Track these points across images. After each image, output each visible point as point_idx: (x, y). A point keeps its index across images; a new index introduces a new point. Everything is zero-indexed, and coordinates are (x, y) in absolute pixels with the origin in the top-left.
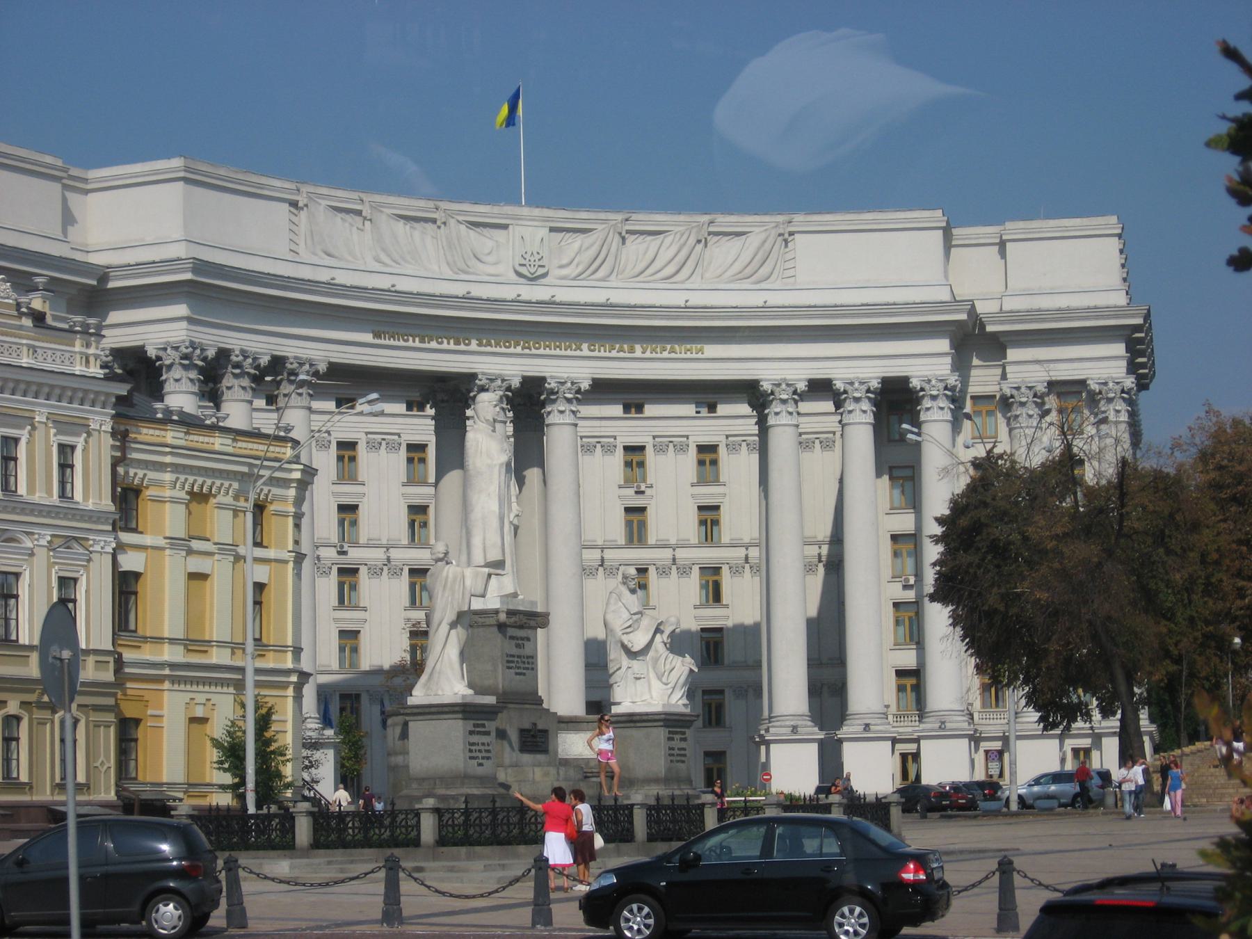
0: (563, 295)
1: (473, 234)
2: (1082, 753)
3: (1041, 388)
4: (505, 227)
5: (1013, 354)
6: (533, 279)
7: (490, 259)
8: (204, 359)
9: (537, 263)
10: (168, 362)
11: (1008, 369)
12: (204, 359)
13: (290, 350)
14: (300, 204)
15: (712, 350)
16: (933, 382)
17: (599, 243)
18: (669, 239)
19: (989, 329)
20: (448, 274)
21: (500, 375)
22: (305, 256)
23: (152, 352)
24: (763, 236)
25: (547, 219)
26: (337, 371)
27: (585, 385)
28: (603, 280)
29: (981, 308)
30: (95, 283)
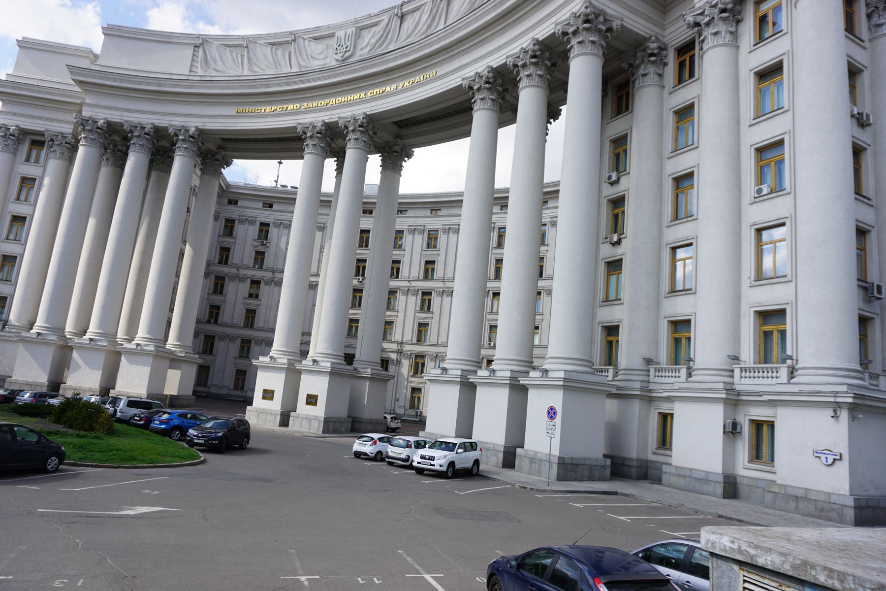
1: (312, 44)
2: (765, 429)
4: (332, 36)
7: (322, 56)
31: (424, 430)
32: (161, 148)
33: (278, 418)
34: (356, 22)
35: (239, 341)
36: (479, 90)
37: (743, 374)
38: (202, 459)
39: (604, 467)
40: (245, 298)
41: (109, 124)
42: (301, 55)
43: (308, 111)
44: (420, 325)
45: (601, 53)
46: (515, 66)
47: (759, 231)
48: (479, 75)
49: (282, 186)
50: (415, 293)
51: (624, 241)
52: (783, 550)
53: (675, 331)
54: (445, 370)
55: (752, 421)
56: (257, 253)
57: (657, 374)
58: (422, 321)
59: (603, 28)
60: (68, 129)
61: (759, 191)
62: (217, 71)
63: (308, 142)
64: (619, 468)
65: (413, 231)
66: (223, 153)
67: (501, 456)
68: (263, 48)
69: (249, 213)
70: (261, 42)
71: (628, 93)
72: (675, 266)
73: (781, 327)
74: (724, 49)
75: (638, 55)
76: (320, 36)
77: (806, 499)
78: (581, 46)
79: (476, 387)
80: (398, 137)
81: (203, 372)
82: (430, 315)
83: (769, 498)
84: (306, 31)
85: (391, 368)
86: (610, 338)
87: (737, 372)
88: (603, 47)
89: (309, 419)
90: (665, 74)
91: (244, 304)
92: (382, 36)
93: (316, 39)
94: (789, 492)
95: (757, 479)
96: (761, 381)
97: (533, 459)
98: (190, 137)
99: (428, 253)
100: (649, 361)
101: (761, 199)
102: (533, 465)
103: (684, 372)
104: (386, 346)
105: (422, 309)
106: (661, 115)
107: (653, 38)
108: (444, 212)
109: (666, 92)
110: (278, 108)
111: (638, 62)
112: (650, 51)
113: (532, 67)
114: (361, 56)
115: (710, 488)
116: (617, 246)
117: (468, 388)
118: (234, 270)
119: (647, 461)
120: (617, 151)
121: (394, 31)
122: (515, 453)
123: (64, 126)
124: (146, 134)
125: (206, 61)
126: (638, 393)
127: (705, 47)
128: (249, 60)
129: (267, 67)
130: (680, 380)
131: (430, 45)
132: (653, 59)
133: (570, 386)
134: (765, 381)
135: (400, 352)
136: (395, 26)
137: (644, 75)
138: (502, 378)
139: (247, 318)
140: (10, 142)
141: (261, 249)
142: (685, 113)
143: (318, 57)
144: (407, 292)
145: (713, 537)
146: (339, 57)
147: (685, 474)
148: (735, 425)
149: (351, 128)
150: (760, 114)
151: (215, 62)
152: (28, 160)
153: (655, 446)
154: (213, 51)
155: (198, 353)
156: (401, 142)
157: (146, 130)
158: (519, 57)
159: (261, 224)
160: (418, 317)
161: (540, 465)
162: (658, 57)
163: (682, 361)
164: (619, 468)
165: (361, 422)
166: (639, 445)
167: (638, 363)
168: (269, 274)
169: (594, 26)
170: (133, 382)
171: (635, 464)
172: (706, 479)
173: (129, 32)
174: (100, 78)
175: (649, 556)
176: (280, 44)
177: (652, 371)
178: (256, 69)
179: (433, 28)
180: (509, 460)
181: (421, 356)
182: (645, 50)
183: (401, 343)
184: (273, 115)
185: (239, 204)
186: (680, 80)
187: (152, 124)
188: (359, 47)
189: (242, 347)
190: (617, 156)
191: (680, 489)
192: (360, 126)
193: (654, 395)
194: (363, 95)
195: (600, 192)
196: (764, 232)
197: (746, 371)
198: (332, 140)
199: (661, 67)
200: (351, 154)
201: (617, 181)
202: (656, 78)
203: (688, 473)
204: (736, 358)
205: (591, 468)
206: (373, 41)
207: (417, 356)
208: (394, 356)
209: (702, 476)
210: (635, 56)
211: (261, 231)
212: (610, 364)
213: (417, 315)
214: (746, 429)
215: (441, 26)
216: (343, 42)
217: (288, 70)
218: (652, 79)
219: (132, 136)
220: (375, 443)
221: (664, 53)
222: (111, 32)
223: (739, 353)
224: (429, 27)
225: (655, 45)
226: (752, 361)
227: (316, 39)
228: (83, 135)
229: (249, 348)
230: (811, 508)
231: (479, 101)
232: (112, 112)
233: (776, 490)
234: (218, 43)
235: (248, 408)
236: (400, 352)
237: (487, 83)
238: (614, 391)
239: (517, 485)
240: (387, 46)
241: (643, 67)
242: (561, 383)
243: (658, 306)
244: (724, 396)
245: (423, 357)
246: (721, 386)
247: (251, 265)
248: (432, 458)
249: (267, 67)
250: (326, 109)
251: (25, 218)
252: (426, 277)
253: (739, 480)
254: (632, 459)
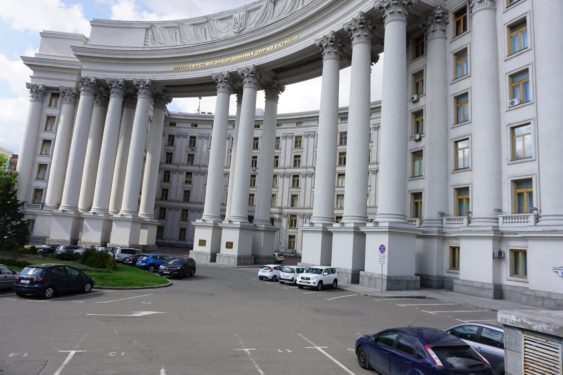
1: (219, 23)
2: (520, 255)
4: (231, 17)
21: (221, 73)
31: (300, 262)
32: (129, 94)
33: (209, 257)
34: (246, 7)
35: (181, 210)
36: (326, 46)
37: (505, 221)
38: (170, 283)
39: (416, 281)
40: (183, 184)
41: (97, 80)
42: (212, 31)
43: (218, 65)
44: (293, 196)
45: (405, 19)
46: (349, 30)
47: (513, 129)
48: (326, 37)
49: (202, 113)
50: (289, 176)
51: (423, 138)
52: (548, 322)
53: (459, 195)
54: (312, 224)
55: (511, 250)
56: (189, 155)
57: (448, 222)
58: (294, 194)
59: (406, 3)
60: (73, 85)
61: (512, 103)
62: (161, 44)
63: (219, 85)
64: (425, 282)
65: (286, 137)
66: (166, 94)
67: (350, 276)
68: (189, 27)
69: (183, 131)
70: (187, 24)
71: (423, 44)
72: (458, 153)
73: (529, 190)
74: (486, 11)
75: (429, 18)
76: (223, 18)
77: (549, 298)
78: (392, 15)
79: (365, 235)
80: (275, 78)
81: (160, 229)
82: (298, 190)
83: (524, 298)
84: (215, 15)
85: (276, 224)
86: (416, 201)
87: (501, 219)
88: (406, 15)
89: (229, 256)
90: (448, 30)
91: (183, 187)
92: (262, 16)
93: (221, 20)
94: (538, 294)
95: (516, 287)
96: (517, 225)
97: (371, 278)
98: (147, 86)
99: (296, 150)
100: (442, 214)
101: (514, 108)
102: (371, 281)
103: (465, 220)
104: (273, 210)
105: (293, 186)
106: (445, 56)
107: (439, 7)
108: (305, 124)
109: (448, 41)
110: (199, 65)
111: (429, 23)
112: (437, 16)
113: (360, 30)
114: (250, 29)
115: (485, 293)
116: (419, 142)
117: (327, 235)
118: (176, 167)
119: (443, 277)
120: (417, 81)
121: (270, 12)
122: (359, 274)
123: (68, 83)
124: (120, 85)
126: (436, 234)
127: (474, 11)
128: (180, 36)
129: (192, 39)
130: (463, 225)
131: (294, 19)
132: (439, 20)
133: (393, 231)
134: (519, 225)
135: (281, 214)
136: (271, 9)
137: (434, 31)
138: (349, 228)
139: (185, 196)
140: (39, 95)
141: (191, 153)
142: (461, 55)
143: (222, 31)
144: (284, 175)
145: (505, 316)
146: (236, 30)
147: (468, 284)
148: (500, 253)
149: (246, 75)
150: (512, 53)
151: (159, 38)
152: (50, 105)
153: (448, 267)
154: (158, 31)
155: (156, 219)
156: (277, 82)
157: (120, 83)
158: (351, 24)
159: (191, 137)
160: (291, 191)
161: (375, 282)
162: (443, 19)
163: (464, 213)
164: (425, 282)
165: (260, 258)
166: (438, 266)
167: (435, 216)
168: (197, 168)
169: (400, 2)
170: (120, 238)
171: (435, 279)
172: (483, 287)
173: (106, 23)
174: (90, 52)
175: (453, 332)
176: (199, 24)
177: (445, 220)
178: (185, 41)
179: (295, 8)
180: (355, 279)
181: (293, 216)
182: (434, 15)
183: (281, 208)
184: (196, 69)
185: (177, 125)
186: (457, 33)
187: (123, 79)
188: (249, 24)
189: (183, 214)
190: (417, 84)
191: (466, 294)
192: (251, 73)
193: (446, 235)
194: (252, 54)
195: (407, 108)
196: (516, 129)
197: (506, 219)
198: (235, 83)
199: (445, 25)
200: (246, 92)
201: (417, 101)
202: (442, 32)
203: (470, 284)
204: (500, 211)
205: (408, 282)
206: (257, 19)
207: (292, 216)
208: (277, 216)
209: (479, 285)
210: (427, 19)
211: (191, 141)
212: (417, 217)
213: (291, 190)
214: (508, 256)
215: (300, 7)
216: (238, 21)
217: (204, 40)
218: (439, 33)
219: (111, 87)
220: (272, 270)
221: (446, 16)
222: (96, 24)
223: (502, 207)
224: (293, 8)
225: (440, 11)
226: (510, 212)
227: (221, 20)
228: (82, 89)
229: (187, 214)
230: (553, 304)
231: (326, 54)
232: (99, 73)
233: (529, 293)
234: (160, 26)
235: (191, 251)
236: (281, 214)
237: (331, 42)
238: (421, 234)
239: (362, 294)
240: (266, 21)
241: (432, 26)
242: (387, 230)
243: (447, 179)
244: (493, 235)
245: (295, 216)
246: (491, 228)
247: (186, 163)
248: (309, 279)
249: (192, 39)
250: (230, 63)
251: (51, 141)
253: (504, 287)
254: (434, 276)
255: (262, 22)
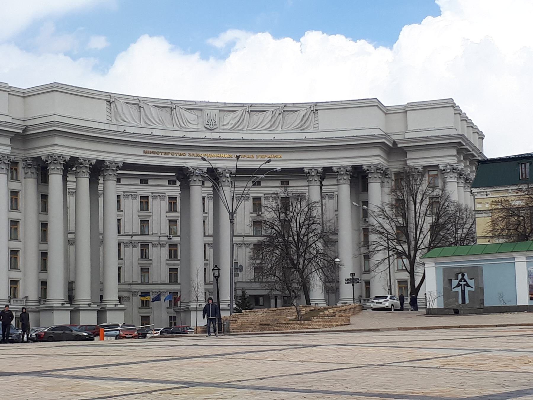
0: (223, 136)
3: (420, 169)
4: (201, 110)
5: (409, 156)
6: (211, 130)
8: (65, 161)
9: (214, 124)
10: (49, 162)
11: (408, 162)
12: (65, 161)
13: (107, 157)
14: (111, 101)
15: (285, 156)
16: (372, 167)
17: (240, 115)
18: (268, 114)
19: (399, 146)
20: (176, 128)
22: (114, 122)
23: (43, 158)
24: (305, 112)
25: (218, 107)
26: (127, 166)
27: (234, 171)
28: (241, 130)
29: (395, 138)
30: (21, 131)
68: (152, 108)
82: (150, 262)
92: (239, 121)
99: (142, 214)
114: (224, 130)
125: (117, 112)
143: (192, 122)
178: (150, 123)
206: (234, 122)
217: (170, 127)
252: (142, 234)
255: (238, 126)
